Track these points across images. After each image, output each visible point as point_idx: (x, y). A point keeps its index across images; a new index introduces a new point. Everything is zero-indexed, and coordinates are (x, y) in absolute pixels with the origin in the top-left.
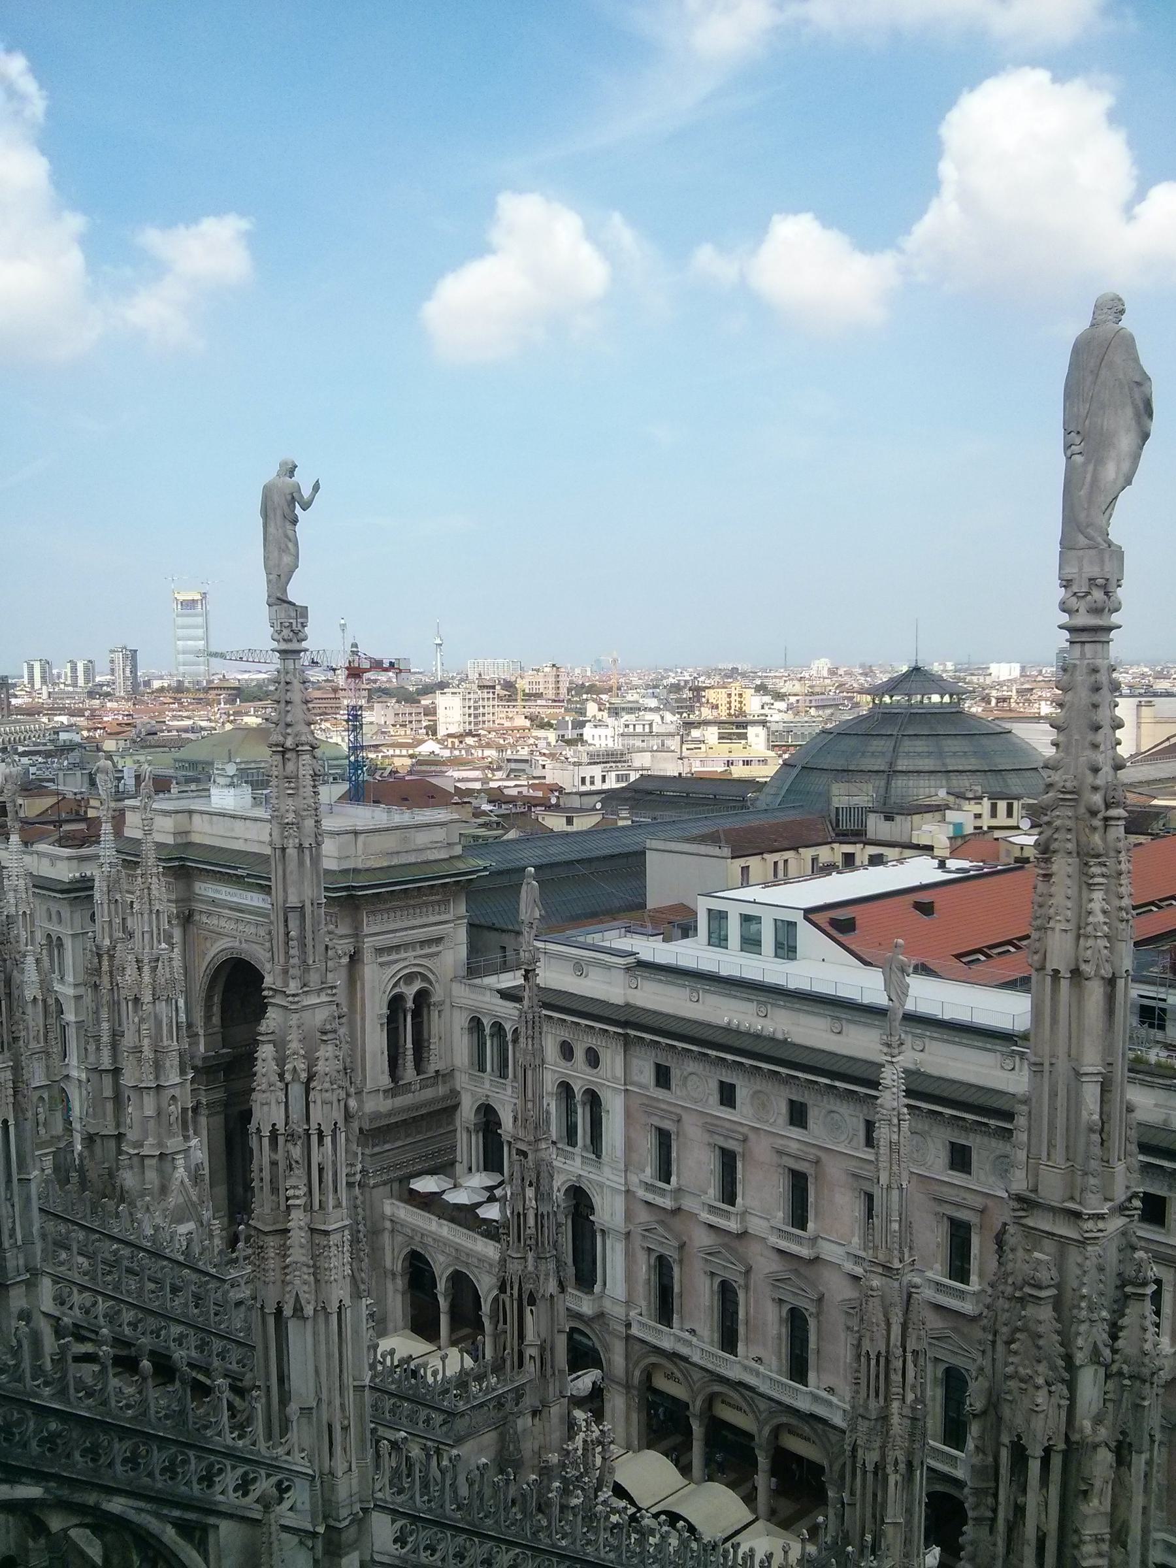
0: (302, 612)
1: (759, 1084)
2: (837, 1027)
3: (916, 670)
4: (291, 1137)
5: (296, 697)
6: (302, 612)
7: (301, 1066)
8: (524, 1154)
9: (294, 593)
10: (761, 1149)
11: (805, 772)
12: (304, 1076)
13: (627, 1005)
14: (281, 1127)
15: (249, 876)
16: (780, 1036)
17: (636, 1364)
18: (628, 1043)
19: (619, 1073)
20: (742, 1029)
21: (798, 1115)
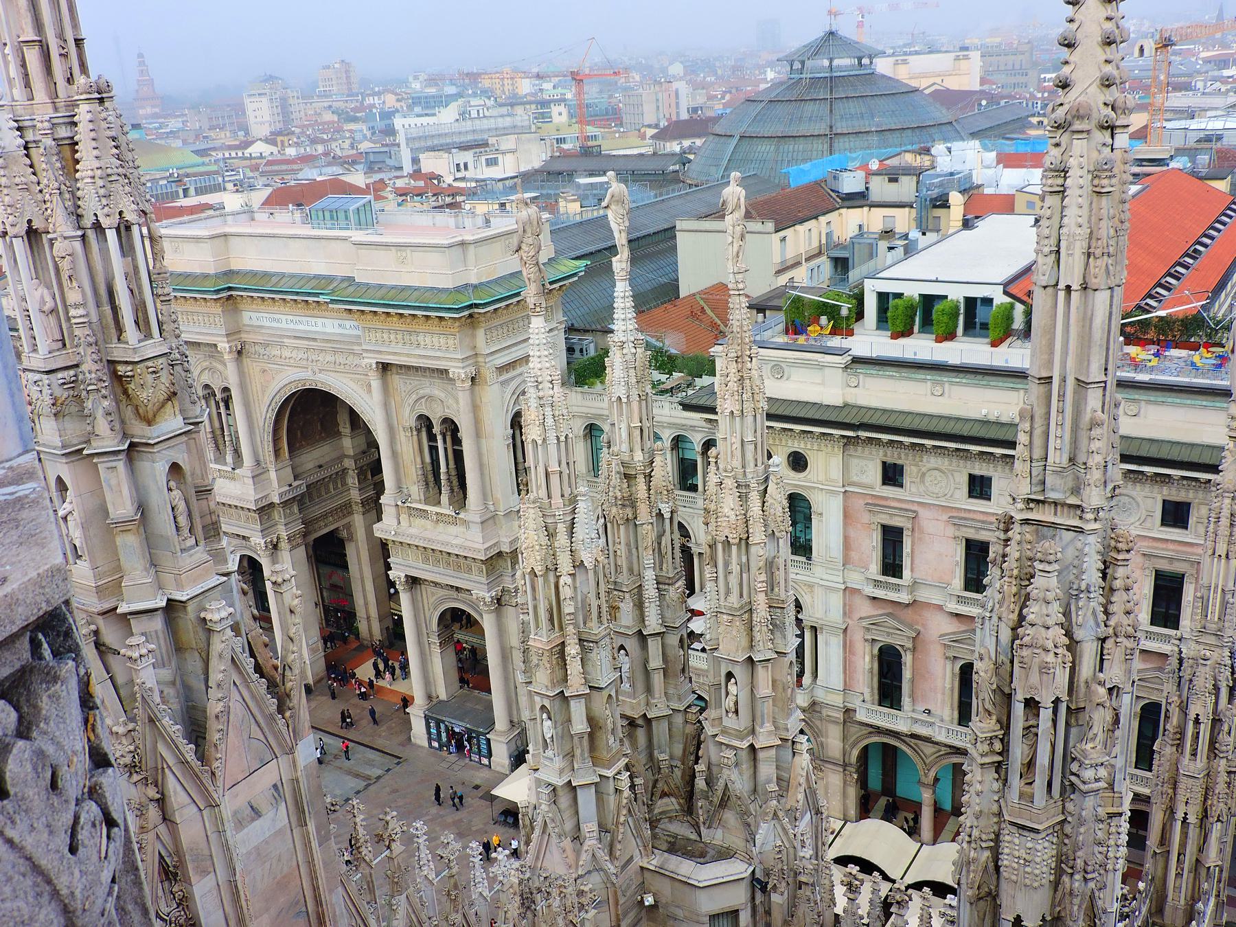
3: (831, 33)
11: (745, 142)
13: (846, 405)
17: (854, 745)
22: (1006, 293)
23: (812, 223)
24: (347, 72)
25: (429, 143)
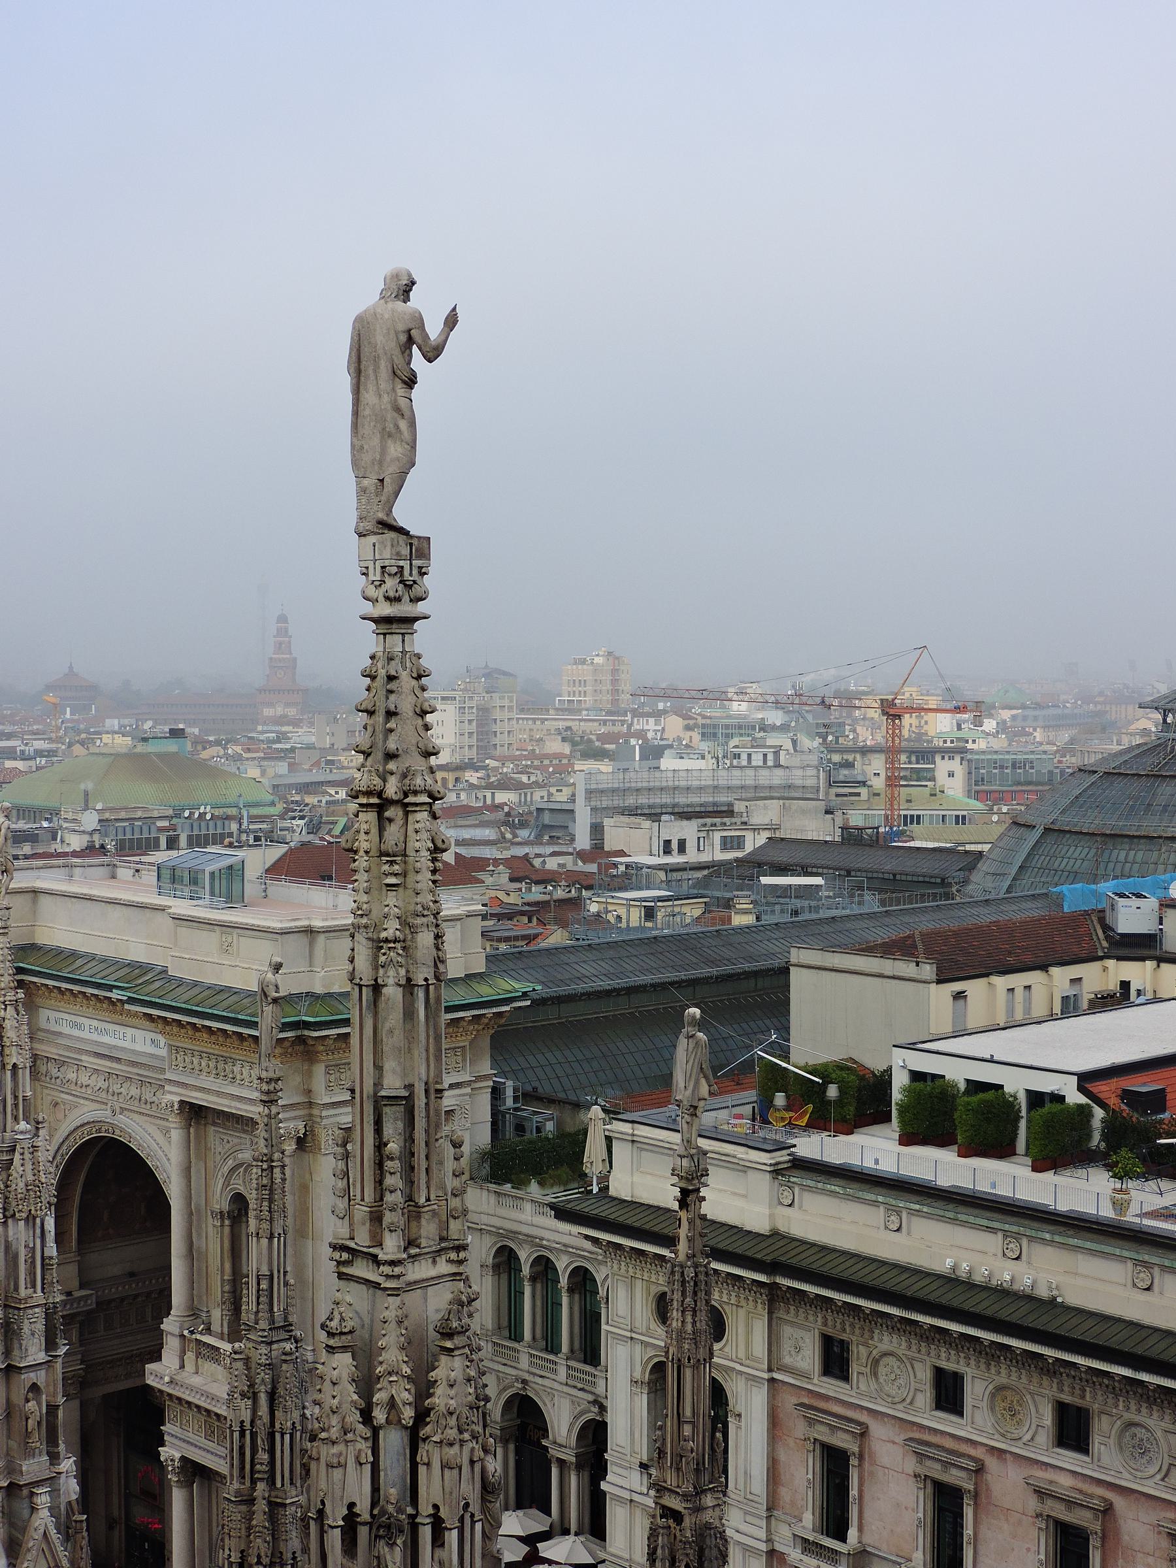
0: (420, 548)
1: (1004, 1375)
2: (1144, 1279)
4: (383, 1528)
5: (405, 704)
6: (420, 548)
7: (404, 1395)
8: (677, 1516)
9: (402, 514)
10: (1007, 1485)
11: (1051, 839)
12: (408, 1414)
13: (775, 1234)
14: (363, 1508)
15: (131, 1001)
16: (1043, 1292)
18: (775, 1297)
19: (760, 1348)
20: (978, 1278)
21: (1072, 1430)
22: (1081, 1089)
23: (1034, 978)
24: (615, 671)
25: (630, 801)
